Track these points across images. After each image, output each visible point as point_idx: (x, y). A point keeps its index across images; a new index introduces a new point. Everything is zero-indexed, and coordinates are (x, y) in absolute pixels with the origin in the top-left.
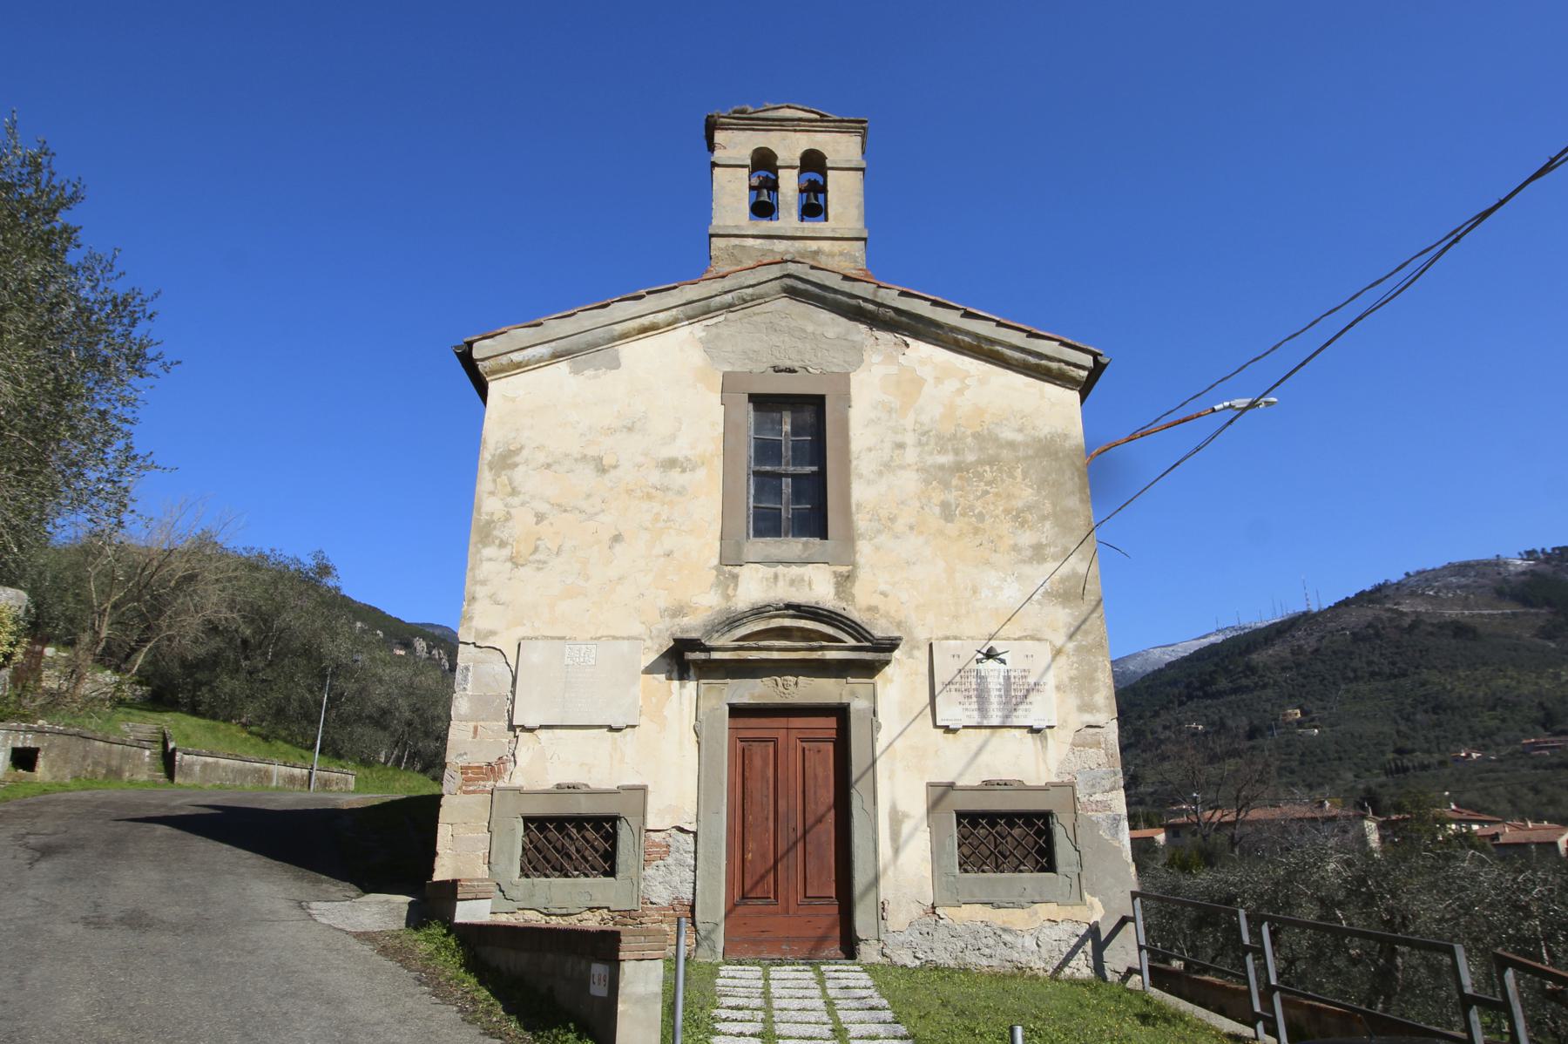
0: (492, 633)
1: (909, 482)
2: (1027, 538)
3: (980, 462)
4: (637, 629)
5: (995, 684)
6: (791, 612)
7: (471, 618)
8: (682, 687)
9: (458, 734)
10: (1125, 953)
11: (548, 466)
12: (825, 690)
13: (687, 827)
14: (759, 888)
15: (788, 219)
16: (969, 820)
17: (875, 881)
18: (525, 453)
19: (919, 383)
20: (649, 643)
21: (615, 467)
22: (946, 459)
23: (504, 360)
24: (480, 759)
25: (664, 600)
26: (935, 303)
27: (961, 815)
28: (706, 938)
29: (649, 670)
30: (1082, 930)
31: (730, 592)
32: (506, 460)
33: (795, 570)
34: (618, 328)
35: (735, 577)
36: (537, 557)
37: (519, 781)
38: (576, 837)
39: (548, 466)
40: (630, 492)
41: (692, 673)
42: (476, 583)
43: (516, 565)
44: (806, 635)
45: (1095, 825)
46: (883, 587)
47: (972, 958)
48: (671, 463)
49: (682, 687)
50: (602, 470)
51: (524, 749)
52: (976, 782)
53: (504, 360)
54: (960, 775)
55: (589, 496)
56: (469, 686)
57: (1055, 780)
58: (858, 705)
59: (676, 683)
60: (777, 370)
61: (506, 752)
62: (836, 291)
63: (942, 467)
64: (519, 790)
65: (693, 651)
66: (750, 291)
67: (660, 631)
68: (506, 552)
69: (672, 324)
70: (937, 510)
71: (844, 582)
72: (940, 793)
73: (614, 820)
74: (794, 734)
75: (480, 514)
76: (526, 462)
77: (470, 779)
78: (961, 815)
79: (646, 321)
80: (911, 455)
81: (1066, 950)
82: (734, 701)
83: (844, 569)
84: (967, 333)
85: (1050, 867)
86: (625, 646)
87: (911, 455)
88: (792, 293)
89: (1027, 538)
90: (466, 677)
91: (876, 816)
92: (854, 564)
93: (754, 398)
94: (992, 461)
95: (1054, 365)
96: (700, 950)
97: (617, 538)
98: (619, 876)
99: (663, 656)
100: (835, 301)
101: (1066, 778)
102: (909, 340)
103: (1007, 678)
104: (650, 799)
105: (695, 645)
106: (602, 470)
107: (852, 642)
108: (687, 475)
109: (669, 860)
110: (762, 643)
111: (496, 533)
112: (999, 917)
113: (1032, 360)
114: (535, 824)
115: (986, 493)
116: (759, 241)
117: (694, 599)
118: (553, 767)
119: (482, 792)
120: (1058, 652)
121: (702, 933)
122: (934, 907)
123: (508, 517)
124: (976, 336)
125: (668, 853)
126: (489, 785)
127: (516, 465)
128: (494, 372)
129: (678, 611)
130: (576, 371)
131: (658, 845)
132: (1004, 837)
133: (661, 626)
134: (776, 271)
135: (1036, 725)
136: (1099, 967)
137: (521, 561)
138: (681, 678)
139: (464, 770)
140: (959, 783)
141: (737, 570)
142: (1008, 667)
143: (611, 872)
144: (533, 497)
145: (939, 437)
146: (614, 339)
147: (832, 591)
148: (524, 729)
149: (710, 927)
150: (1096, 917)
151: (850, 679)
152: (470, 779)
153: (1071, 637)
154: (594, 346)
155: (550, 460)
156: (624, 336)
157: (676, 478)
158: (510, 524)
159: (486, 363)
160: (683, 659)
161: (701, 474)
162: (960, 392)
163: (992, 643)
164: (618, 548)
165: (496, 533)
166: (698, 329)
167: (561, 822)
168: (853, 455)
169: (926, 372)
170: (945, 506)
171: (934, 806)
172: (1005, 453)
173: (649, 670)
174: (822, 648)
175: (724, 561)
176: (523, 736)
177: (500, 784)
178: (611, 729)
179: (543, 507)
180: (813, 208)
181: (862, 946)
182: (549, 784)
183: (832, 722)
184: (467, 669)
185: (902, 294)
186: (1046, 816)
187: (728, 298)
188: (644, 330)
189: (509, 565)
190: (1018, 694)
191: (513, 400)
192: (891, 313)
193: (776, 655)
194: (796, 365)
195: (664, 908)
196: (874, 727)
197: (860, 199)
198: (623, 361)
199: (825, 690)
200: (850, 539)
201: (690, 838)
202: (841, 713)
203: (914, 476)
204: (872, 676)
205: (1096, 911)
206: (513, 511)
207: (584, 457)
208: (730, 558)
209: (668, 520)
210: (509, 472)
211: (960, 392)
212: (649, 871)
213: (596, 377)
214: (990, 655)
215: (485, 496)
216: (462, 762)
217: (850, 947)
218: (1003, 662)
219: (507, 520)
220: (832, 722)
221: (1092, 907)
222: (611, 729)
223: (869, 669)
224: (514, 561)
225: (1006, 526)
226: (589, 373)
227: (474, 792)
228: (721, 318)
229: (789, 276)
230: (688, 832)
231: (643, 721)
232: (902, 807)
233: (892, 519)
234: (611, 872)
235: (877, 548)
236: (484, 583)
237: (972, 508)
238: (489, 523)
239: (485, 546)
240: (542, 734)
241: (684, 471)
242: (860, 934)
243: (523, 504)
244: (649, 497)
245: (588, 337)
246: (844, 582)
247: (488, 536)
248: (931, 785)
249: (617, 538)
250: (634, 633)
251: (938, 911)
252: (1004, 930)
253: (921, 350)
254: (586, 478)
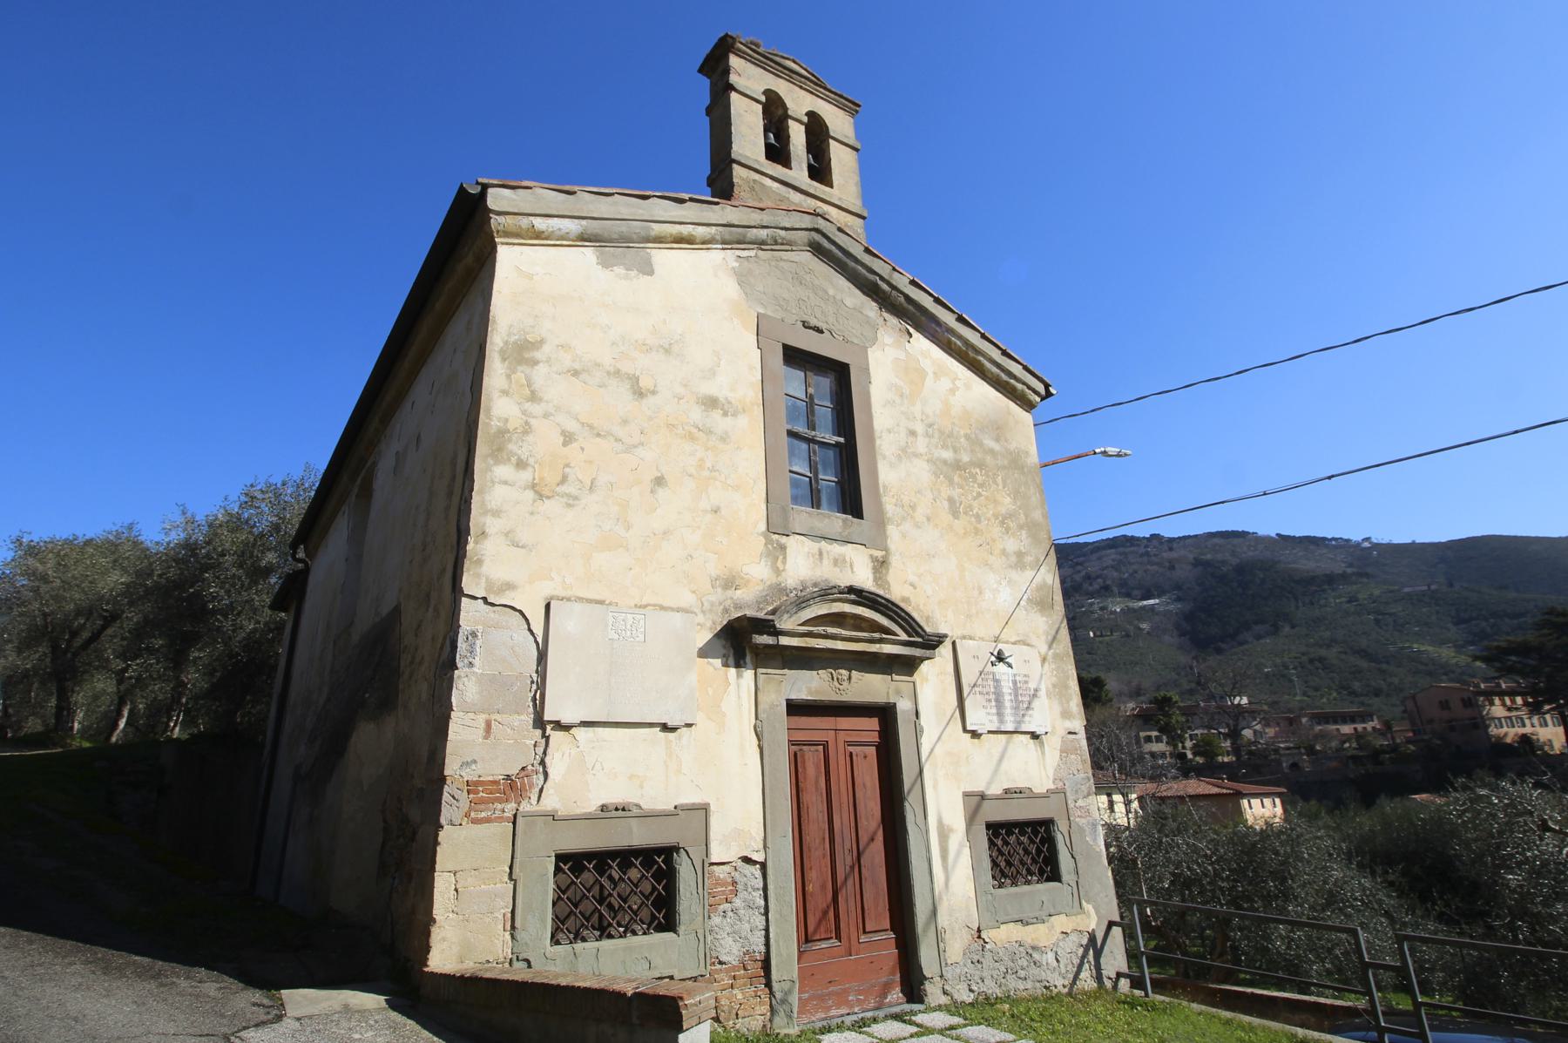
0: (509, 586)
1: (921, 471)
2: (1012, 545)
3: (973, 464)
4: (687, 599)
5: (1007, 688)
6: (853, 597)
7: (480, 562)
8: (739, 676)
9: (462, 732)
10: (1115, 959)
11: (576, 373)
12: (869, 687)
13: (755, 857)
14: (822, 929)
15: (799, 172)
16: (997, 830)
17: (934, 912)
18: (546, 348)
19: (922, 374)
20: (700, 618)
21: (654, 393)
22: (947, 455)
23: (524, 222)
24: (494, 767)
25: (714, 568)
26: (937, 301)
27: (989, 826)
28: (784, 1001)
29: (704, 653)
30: (1085, 941)
31: (779, 564)
32: (523, 352)
33: (837, 549)
34: (657, 229)
35: (783, 548)
36: (563, 489)
37: (550, 802)
38: (624, 880)
39: (576, 373)
40: (670, 427)
41: (748, 659)
42: (486, 513)
43: (541, 496)
44: (858, 623)
45: (1081, 830)
46: (912, 578)
47: (1013, 984)
48: (711, 403)
49: (739, 676)
50: (640, 394)
51: (557, 755)
52: (999, 792)
53: (524, 222)
54: (989, 783)
55: (625, 422)
56: (477, 661)
57: (1052, 787)
58: (904, 706)
59: (733, 671)
60: (806, 325)
61: (530, 758)
62: (857, 261)
63: (945, 462)
64: (553, 816)
65: (761, 634)
66: (783, 233)
67: (712, 604)
68: (526, 476)
69: (707, 242)
70: (946, 504)
71: (881, 565)
72: (976, 801)
73: (669, 852)
74: (842, 736)
75: (489, 417)
76: (548, 361)
77: (482, 801)
78: (989, 826)
79: (686, 230)
80: (921, 445)
81: (1076, 961)
82: (793, 697)
83: (879, 554)
84: (960, 337)
85: (1055, 876)
86: (678, 618)
87: (921, 445)
88: (817, 250)
89: (1012, 545)
90: (472, 646)
91: (927, 831)
92: (886, 549)
93: (786, 348)
94: (981, 465)
95: (1019, 386)
96: (777, 1020)
97: (659, 481)
98: (681, 929)
99: (717, 636)
100: (855, 270)
101: (1060, 785)
102: (912, 330)
103: (1015, 682)
104: (713, 821)
105: (766, 626)
106: (640, 394)
107: (904, 637)
108: (729, 419)
109: (738, 902)
110: (831, 630)
111: (511, 446)
112: (1029, 934)
113: (1004, 377)
114: (570, 863)
115: (979, 495)
116: (776, 185)
117: (745, 569)
118: (600, 780)
119: (500, 819)
120: (1044, 660)
121: (779, 995)
122: (979, 931)
123: (527, 429)
124: (966, 342)
125: (736, 893)
126: (510, 808)
127: (535, 363)
128: (507, 234)
129: (730, 582)
130: (605, 264)
131: (724, 884)
132: (1022, 847)
133: (713, 598)
134: (807, 221)
136: (1099, 978)
137: (546, 492)
138: (738, 666)
139: (472, 787)
140: (989, 792)
141: (784, 540)
142: (1014, 671)
143: (668, 924)
144: (558, 409)
145: (941, 432)
146: (648, 240)
147: (871, 577)
148: (558, 726)
149: (786, 986)
150: (1093, 926)
151: (896, 677)
152: (482, 801)
153: (1050, 647)
154: (625, 241)
155: (577, 366)
156: (659, 240)
157: (717, 420)
158: (530, 438)
159: (501, 219)
160: (742, 641)
161: (742, 421)
162: (953, 391)
163: (1000, 646)
164: (660, 491)
165: (511, 446)
166: (730, 255)
167: (601, 859)
168: (877, 434)
169: (926, 364)
170: (951, 500)
171: (971, 820)
172: (989, 459)
173: (704, 653)
174: (881, 641)
175: (770, 529)
176: (556, 736)
177: (525, 807)
178: (665, 728)
179: (571, 426)
180: (820, 171)
181: (928, 986)
182: (592, 806)
183: (873, 723)
184: (474, 634)
185: (913, 283)
186: (1048, 824)
187: (763, 233)
188: (680, 240)
189: (530, 494)
190: (1024, 702)
191: (530, 277)
192: (902, 299)
193: (840, 645)
194: (823, 326)
195: (734, 968)
196: (918, 732)
197: (857, 178)
198: (656, 267)
199: (869, 687)
200: (881, 523)
201: (756, 870)
202: (885, 714)
203: (925, 465)
204: (911, 675)
205: (1091, 921)
206: (533, 422)
207: (617, 372)
208: (777, 527)
209: (713, 469)
210: (527, 370)
211: (953, 391)
212: (716, 920)
213: (626, 277)
214: (1000, 658)
215: (495, 395)
216: (469, 774)
217: (913, 987)
218: (1010, 666)
219: (526, 433)
220: (873, 723)
221: (1089, 916)
222: (665, 728)
223: (907, 666)
224: (539, 491)
225: (996, 530)
226: (620, 270)
227: (487, 820)
228: (752, 253)
229: (817, 230)
230: (754, 862)
231: (699, 719)
232: (947, 821)
233: (913, 507)
234: (668, 924)
235: (904, 536)
236: (497, 513)
237: (971, 507)
238: (502, 432)
239: (498, 462)
240: (580, 733)
241: (725, 414)
242: (927, 973)
243: (546, 416)
244: (692, 438)
245: (623, 227)
246: (881, 565)
247: (500, 449)
248: (966, 795)
249: (659, 481)
250: (683, 604)
251: (984, 935)
252: (1033, 948)
253: (920, 342)
254: (619, 399)
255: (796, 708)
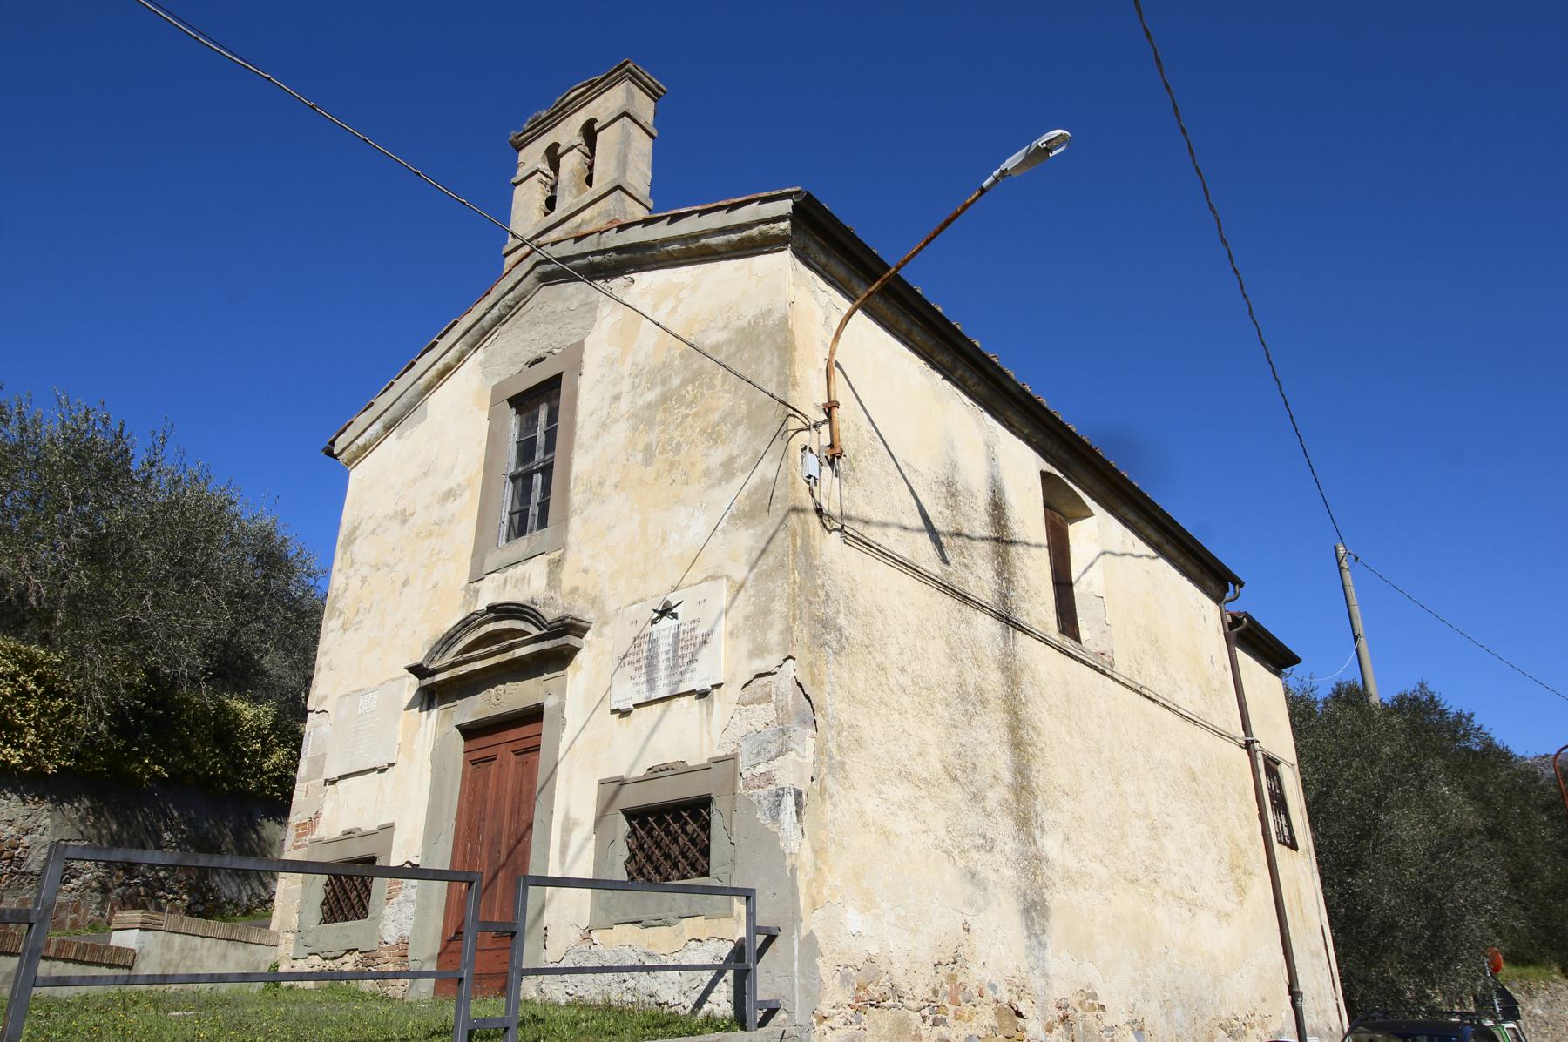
2: (718, 455)
5: (664, 646)
6: (491, 615)
27: (630, 814)
29: (409, 707)
45: (752, 806)
53: (354, 448)
58: (550, 703)
69: (461, 359)
79: (439, 366)
83: (555, 555)
88: (547, 279)
95: (754, 232)
97: (405, 584)
107: (535, 632)
113: (735, 237)
135: (699, 687)
173: (409, 707)
174: (512, 647)
182: (337, 833)
187: (495, 311)
190: (687, 650)
192: (614, 255)
193: (479, 665)
223: (560, 659)
232: (573, 815)
248: (603, 783)
249: (405, 584)
255: (470, 732)
